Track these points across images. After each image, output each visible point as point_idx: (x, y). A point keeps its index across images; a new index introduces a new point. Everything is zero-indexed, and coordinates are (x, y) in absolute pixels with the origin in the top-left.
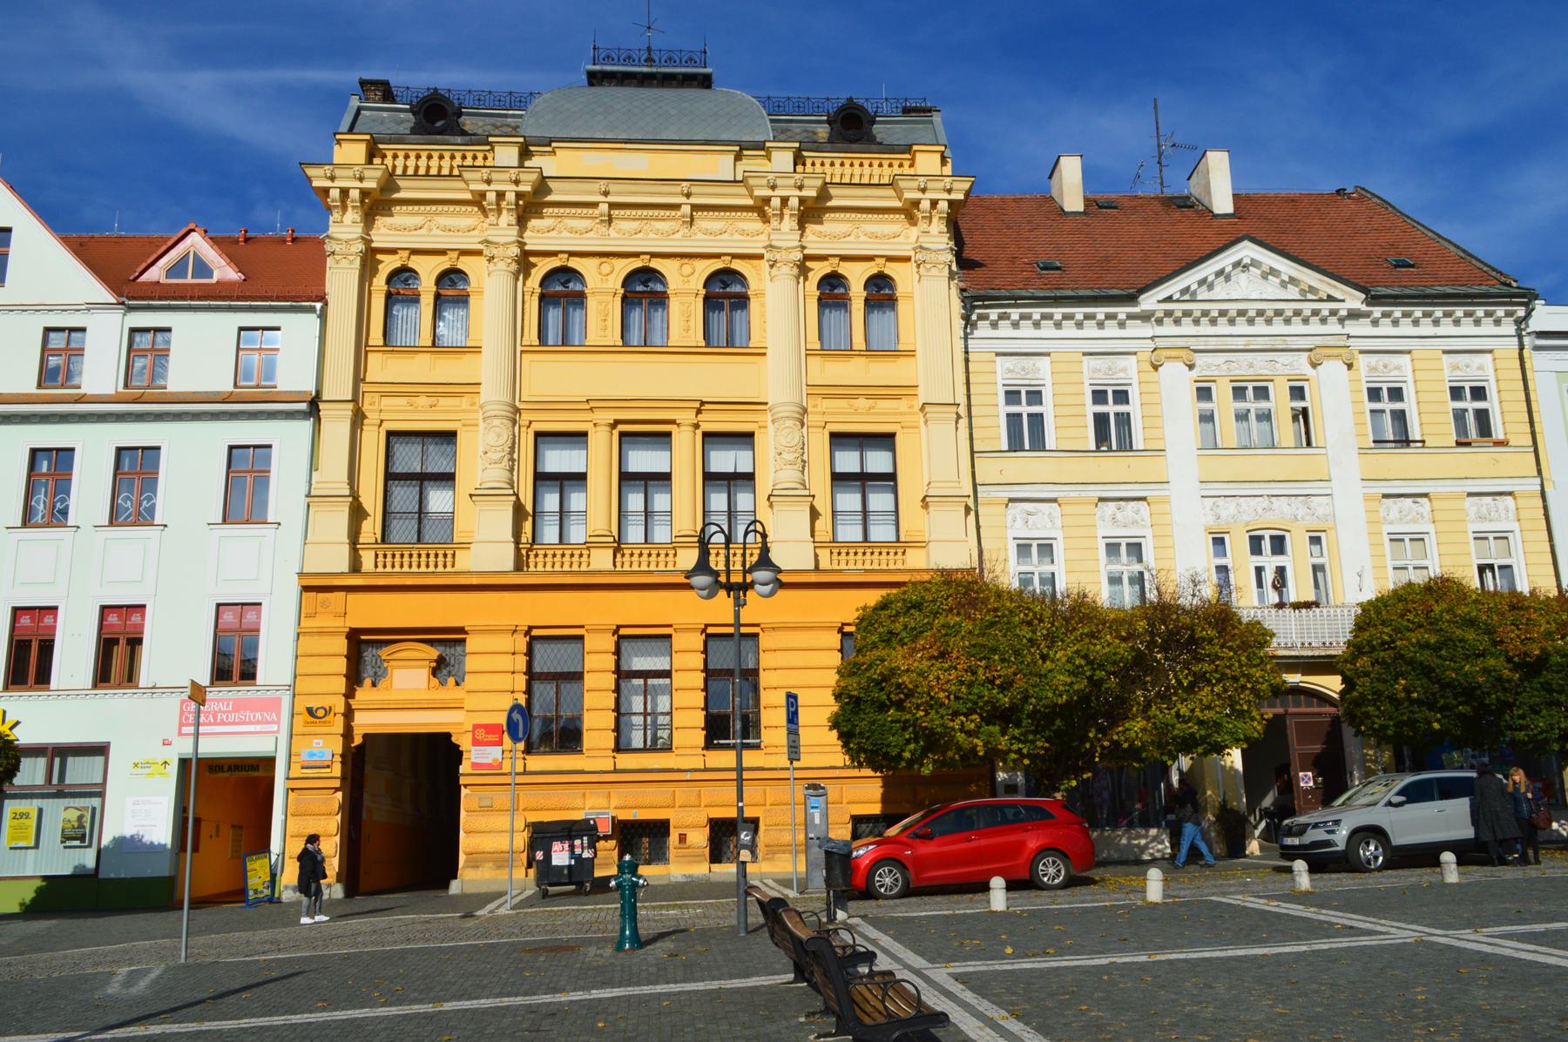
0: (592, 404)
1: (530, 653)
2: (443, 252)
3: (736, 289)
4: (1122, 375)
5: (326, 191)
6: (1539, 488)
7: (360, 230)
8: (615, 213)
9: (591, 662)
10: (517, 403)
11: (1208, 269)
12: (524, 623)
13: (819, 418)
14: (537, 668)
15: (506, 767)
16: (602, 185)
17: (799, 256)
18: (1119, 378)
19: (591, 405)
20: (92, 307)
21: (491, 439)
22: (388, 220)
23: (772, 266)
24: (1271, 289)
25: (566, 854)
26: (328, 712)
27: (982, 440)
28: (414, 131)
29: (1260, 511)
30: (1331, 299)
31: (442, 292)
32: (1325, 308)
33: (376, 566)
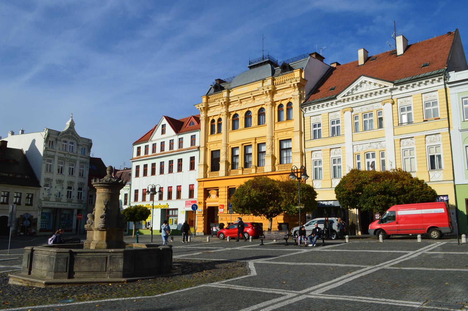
2: (217, 115)
5: (198, 109)
8: (242, 101)
11: (353, 86)
12: (227, 186)
15: (224, 213)
16: (237, 97)
18: (337, 117)
19: (238, 141)
20: (174, 136)
22: (210, 111)
24: (372, 87)
25: (215, 229)
26: (201, 203)
30: (385, 87)
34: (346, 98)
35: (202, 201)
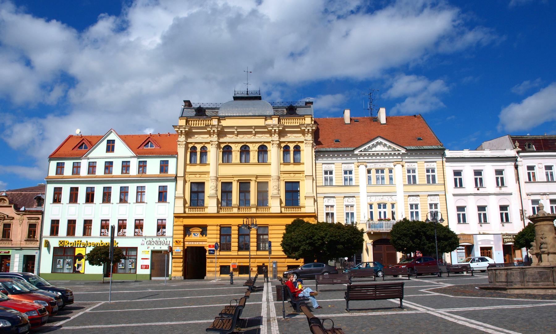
0: (233, 176)
1: (220, 230)
3: (264, 149)
4: (351, 168)
6: (444, 193)
7: (185, 139)
9: (233, 232)
10: (218, 176)
11: (370, 144)
13: (283, 178)
14: (222, 234)
17: (278, 142)
19: (233, 177)
20: (131, 157)
21: (212, 184)
23: (272, 145)
26: (180, 242)
27: (318, 183)
28: (196, 115)
29: (381, 199)
30: (398, 150)
31: (202, 151)
32: (397, 153)
33: (189, 211)
34: (363, 153)
35: (182, 240)
